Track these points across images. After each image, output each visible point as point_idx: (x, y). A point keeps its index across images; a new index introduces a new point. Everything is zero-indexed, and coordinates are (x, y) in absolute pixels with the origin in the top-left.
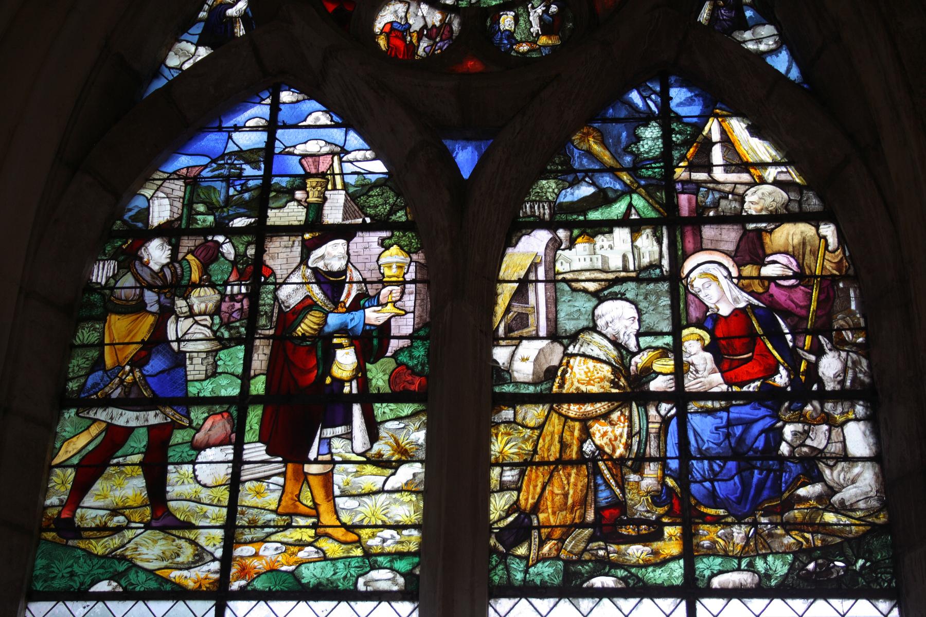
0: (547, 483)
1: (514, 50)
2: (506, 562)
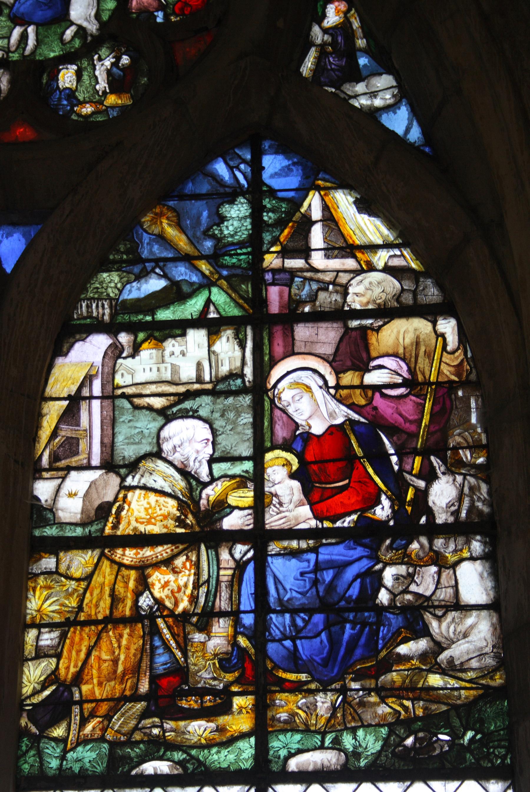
0: (93, 647)
1: (75, 112)
2: (38, 746)
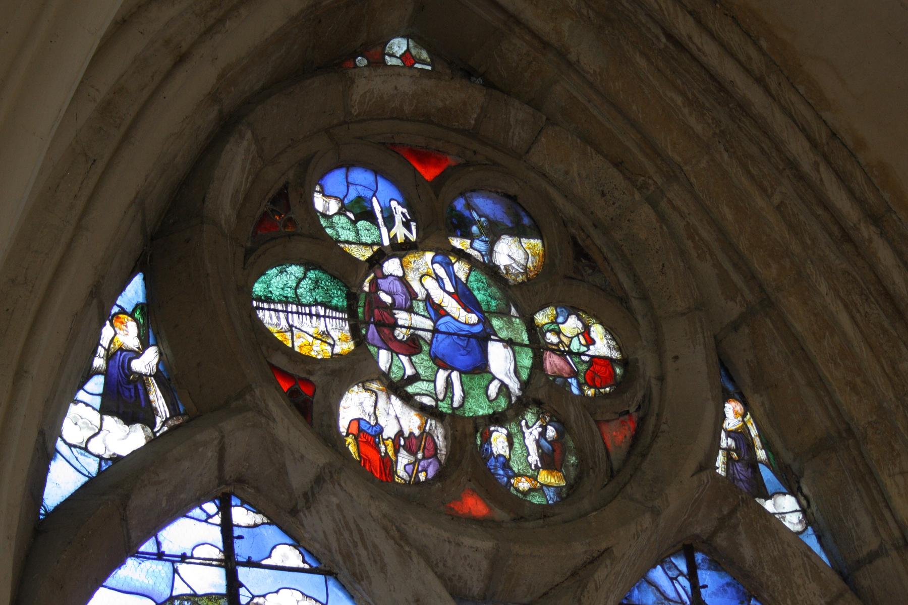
1: (513, 485)
